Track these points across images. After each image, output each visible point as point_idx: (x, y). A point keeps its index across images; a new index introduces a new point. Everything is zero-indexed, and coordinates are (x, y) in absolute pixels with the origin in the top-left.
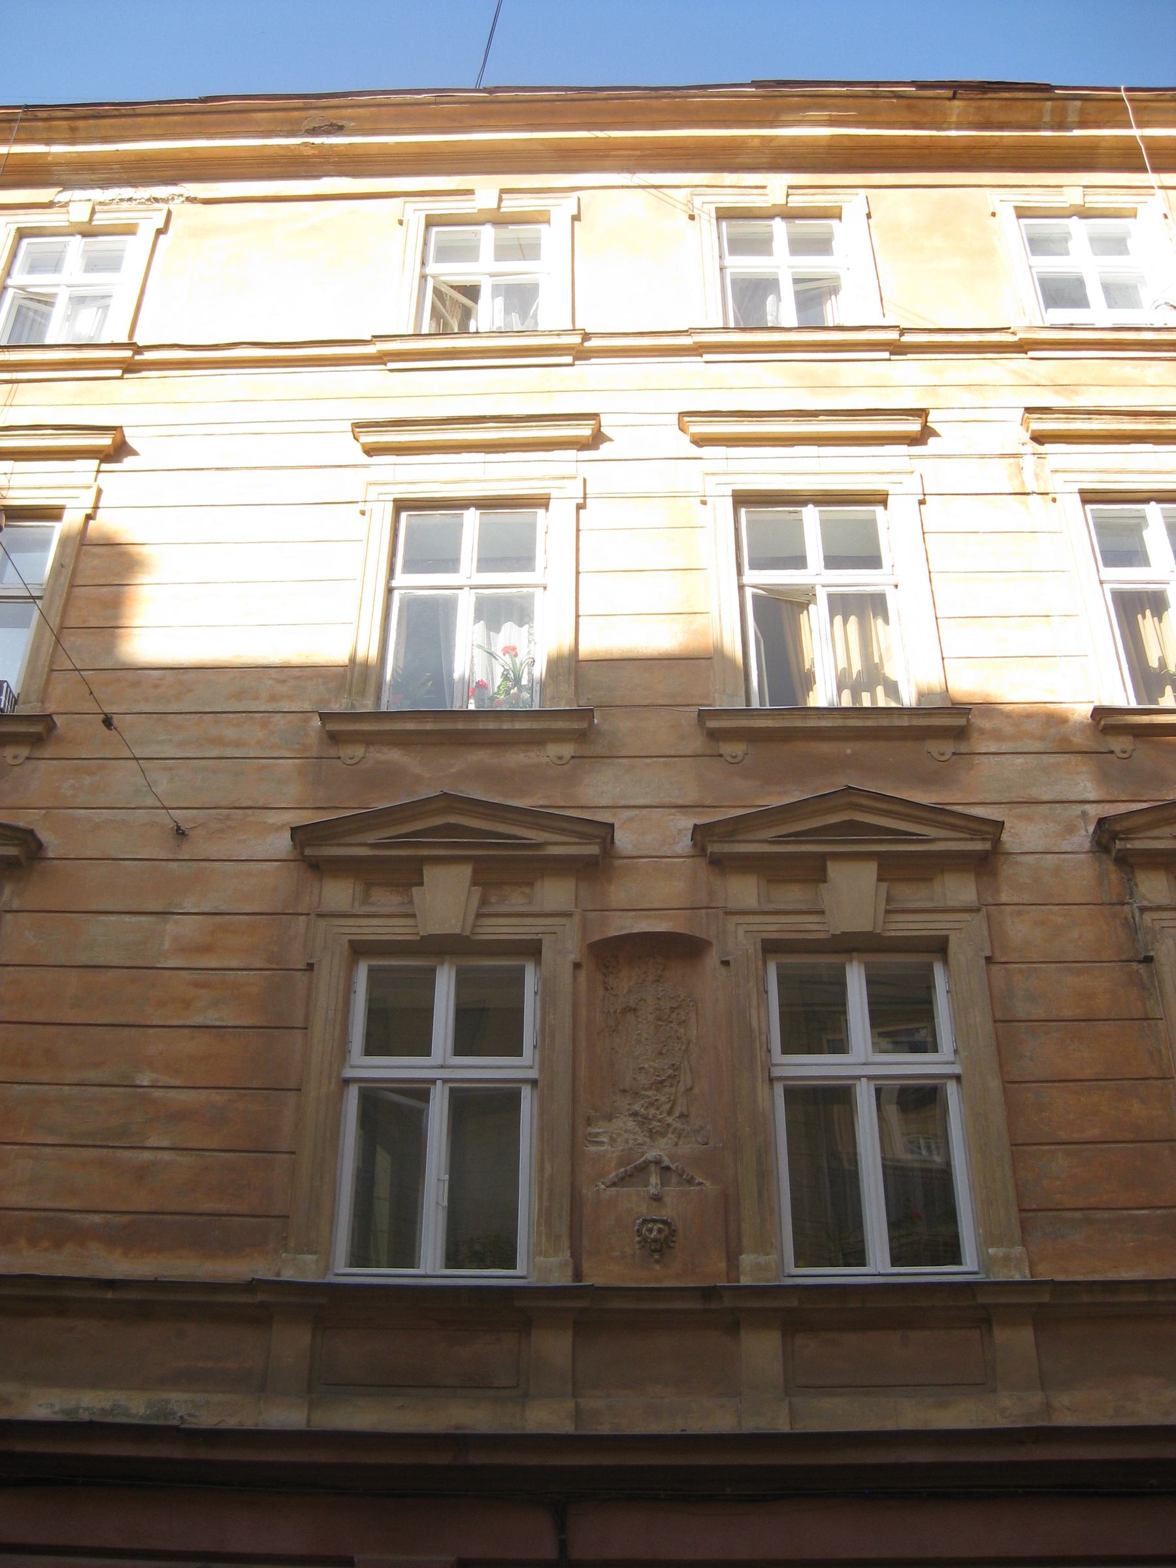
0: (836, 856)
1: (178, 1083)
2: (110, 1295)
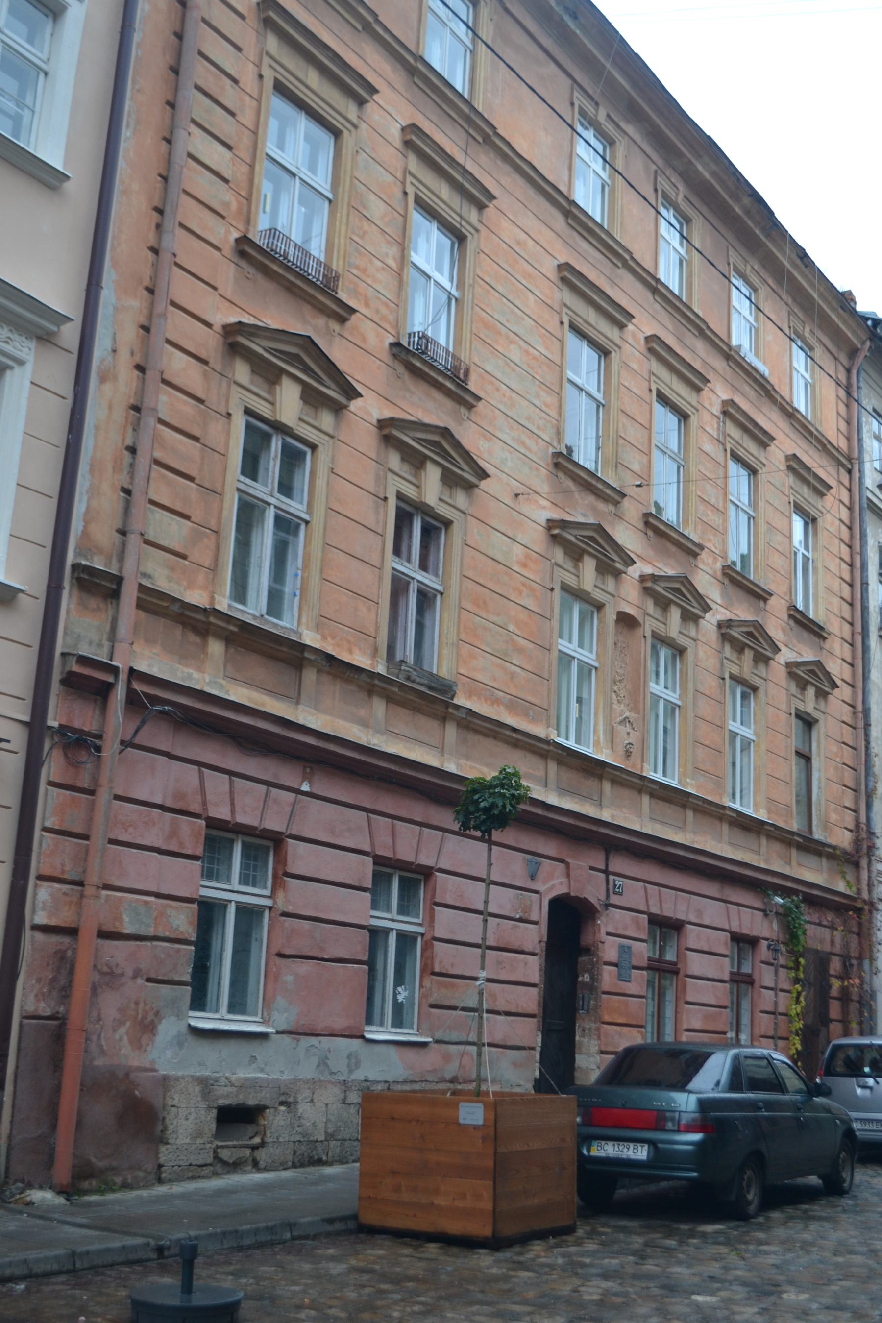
1: (519, 633)
2: (514, 735)
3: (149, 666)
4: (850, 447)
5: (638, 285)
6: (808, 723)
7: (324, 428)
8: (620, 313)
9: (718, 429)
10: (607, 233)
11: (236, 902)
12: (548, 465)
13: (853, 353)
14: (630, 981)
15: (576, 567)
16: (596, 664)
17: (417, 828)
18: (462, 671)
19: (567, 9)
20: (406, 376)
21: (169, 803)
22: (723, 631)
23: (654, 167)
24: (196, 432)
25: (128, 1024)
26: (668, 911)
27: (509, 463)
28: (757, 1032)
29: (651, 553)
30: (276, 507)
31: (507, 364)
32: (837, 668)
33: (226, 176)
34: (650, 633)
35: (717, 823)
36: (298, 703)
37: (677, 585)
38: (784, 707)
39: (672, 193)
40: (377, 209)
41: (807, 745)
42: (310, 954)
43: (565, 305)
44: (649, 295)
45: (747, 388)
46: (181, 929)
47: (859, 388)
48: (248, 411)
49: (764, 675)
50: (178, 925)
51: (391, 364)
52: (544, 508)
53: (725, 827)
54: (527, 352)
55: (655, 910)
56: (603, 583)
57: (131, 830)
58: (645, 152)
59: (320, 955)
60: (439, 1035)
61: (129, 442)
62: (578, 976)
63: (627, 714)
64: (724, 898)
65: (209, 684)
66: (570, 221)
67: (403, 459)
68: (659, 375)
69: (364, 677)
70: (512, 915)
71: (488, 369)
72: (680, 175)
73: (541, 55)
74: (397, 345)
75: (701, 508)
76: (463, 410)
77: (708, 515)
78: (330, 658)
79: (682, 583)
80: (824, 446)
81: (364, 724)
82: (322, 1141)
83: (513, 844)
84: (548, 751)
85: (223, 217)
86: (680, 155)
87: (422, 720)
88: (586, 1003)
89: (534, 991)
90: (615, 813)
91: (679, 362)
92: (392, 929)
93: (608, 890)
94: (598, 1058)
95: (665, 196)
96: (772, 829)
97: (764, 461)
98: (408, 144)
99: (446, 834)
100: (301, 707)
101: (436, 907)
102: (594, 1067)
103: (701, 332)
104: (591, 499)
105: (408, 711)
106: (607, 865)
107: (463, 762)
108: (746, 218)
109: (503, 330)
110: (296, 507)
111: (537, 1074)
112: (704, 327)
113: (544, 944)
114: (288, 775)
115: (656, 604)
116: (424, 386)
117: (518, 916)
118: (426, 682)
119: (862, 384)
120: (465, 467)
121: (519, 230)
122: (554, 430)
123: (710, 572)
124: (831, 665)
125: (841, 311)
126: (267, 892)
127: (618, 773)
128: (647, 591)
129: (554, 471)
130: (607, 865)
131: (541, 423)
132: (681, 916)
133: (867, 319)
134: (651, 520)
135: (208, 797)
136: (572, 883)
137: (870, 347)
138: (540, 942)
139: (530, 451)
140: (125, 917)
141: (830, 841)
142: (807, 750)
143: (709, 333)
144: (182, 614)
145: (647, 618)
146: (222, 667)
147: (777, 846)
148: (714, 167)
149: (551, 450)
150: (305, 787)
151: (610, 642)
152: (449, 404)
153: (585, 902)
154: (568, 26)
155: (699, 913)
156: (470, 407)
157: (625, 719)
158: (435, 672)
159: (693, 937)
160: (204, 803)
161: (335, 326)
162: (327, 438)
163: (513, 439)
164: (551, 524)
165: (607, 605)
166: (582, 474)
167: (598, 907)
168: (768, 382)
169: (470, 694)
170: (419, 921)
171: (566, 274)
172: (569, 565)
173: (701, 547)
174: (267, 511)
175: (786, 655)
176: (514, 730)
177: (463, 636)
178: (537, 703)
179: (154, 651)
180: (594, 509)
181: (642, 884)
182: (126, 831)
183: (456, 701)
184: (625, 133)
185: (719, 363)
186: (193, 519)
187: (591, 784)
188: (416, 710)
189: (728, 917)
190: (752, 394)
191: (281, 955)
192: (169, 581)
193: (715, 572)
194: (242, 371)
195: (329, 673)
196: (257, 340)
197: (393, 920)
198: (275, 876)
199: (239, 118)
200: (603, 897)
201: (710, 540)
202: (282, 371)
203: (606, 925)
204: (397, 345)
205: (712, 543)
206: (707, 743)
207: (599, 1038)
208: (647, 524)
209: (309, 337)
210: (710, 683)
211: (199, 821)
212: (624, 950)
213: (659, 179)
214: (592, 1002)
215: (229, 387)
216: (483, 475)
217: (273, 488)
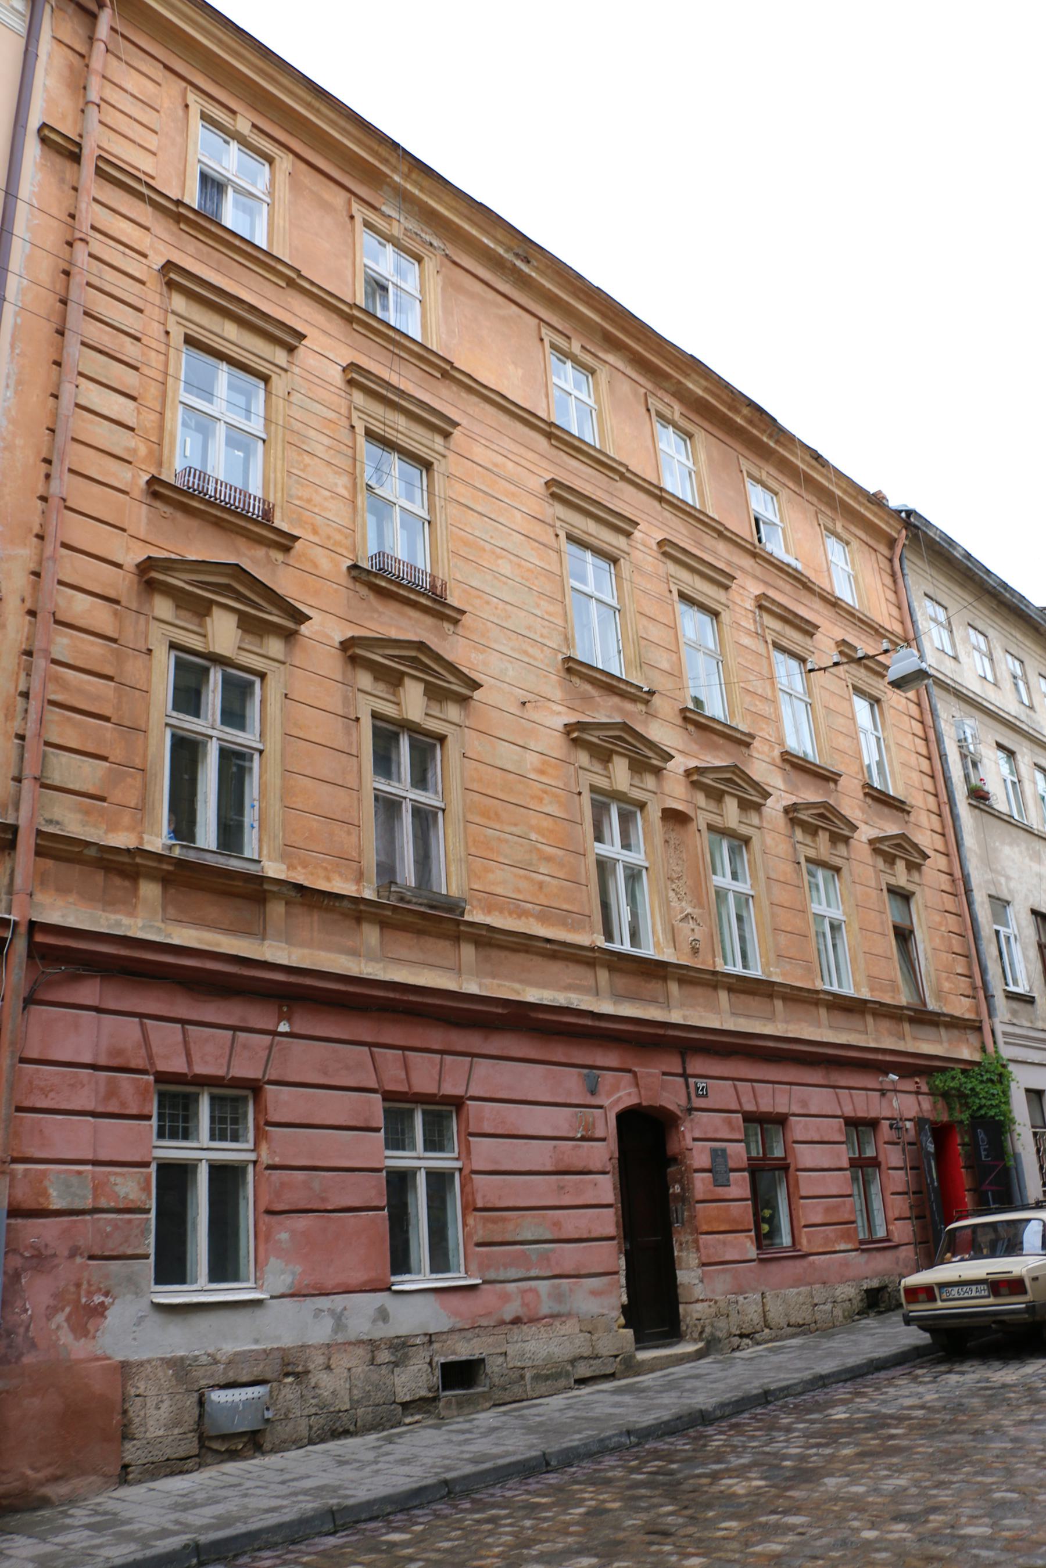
1: (544, 841)
2: (548, 946)
3: (63, 916)
4: (905, 630)
5: (643, 497)
6: (903, 896)
7: (271, 654)
8: (623, 522)
9: (755, 621)
10: (600, 451)
11: (207, 1160)
12: (558, 671)
13: (891, 543)
15: (606, 768)
16: (646, 864)
17: (437, 1057)
18: (475, 887)
19: (517, 255)
20: (372, 597)
21: (103, 1061)
22: (791, 816)
23: (643, 391)
24: (108, 671)
25: (68, 1310)
26: (766, 1106)
27: (511, 673)
28: (890, 1215)
29: (694, 747)
30: (219, 739)
31: (497, 578)
32: (925, 840)
33: (130, 424)
34: (705, 826)
35: (813, 1009)
36: (263, 939)
37: (728, 775)
38: (873, 884)
39: (667, 412)
40: (319, 443)
41: (908, 918)
42: (309, 1207)
43: (558, 518)
44: (656, 504)
45: (781, 583)
46: (131, 1197)
47: (903, 575)
48: (173, 646)
49: (845, 854)
50: (127, 1194)
51: (351, 586)
52: (559, 713)
53: (823, 1012)
54: (519, 565)
55: (749, 1107)
56: (642, 782)
57: (52, 1095)
58: (630, 377)
59: (322, 1207)
60: (492, 1275)
61: (22, 687)
62: (668, 1189)
63: (689, 910)
64: (832, 1084)
65: (143, 928)
66: (553, 442)
67: (376, 679)
68: (678, 576)
69: (346, 903)
70: (571, 1135)
71: (473, 584)
72: (674, 395)
73: (500, 299)
74: (355, 567)
75: (748, 699)
76: (446, 625)
77: (756, 705)
78: (299, 888)
79: (734, 773)
80: (876, 631)
81: (354, 953)
82: (346, 1411)
83: (563, 1060)
84: (595, 958)
85: (130, 463)
86: (667, 377)
87: (430, 942)
88: (680, 1216)
89: (612, 1210)
90: (687, 1013)
91: (698, 563)
92: (420, 1168)
93: (689, 1094)
94: (700, 1271)
95: (659, 415)
96: (877, 1006)
97: (812, 649)
98: (351, 382)
99: (475, 1059)
100: (267, 943)
101: (471, 1139)
102: (697, 1281)
103: (720, 534)
104: (616, 700)
105: (410, 935)
106: (684, 1068)
107: (487, 981)
108: (750, 428)
109: (488, 546)
110: (246, 738)
111: (624, 1299)
112: (722, 529)
113: (615, 1162)
114: (258, 1016)
115: (708, 796)
116: (396, 606)
117: (579, 1135)
118: (425, 901)
119: (906, 571)
120: (452, 679)
121: (495, 454)
122: (562, 637)
123: (768, 760)
124: (920, 837)
125: (869, 505)
126: (250, 1145)
127: (684, 972)
128: (695, 784)
129: (567, 677)
130: (684, 1068)
131: (545, 631)
132: (782, 1109)
133: (901, 511)
134: (689, 714)
135: (155, 1050)
136: (643, 1092)
137: (907, 536)
138: (610, 1159)
139: (535, 659)
140: (51, 1191)
141: (945, 1010)
142: (908, 923)
143: (729, 534)
144: (102, 859)
145: (699, 811)
146: (160, 910)
147: (885, 1024)
148: (704, 383)
149: (560, 657)
150: (284, 1027)
151: (658, 839)
152: (429, 621)
153: (662, 1109)
154: (521, 270)
155: (804, 1103)
156: (456, 622)
157: (686, 916)
158: (444, 892)
159: (799, 1128)
160: (150, 1057)
161: (278, 556)
162: (276, 664)
163: (512, 649)
164: (569, 728)
165: (649, 803)
166: (598, 676)
167: (679, 1113)
168: (802, 574)
169: (489, 910)
170: (456, 1155)
171: (554, 489)
172: (597, 767)
173: (752, 736)
174: (209, 745)
175: (865, 833)
176: (548, 941)
177: (473, 851)
178: (575, 910)
179: (71, 900)
180: (620, 710)
181: (731, 1082)
182: (47, 1096)
183: (467, 918)
184: (606, 362)
185: (747, 562)
186: (111, 759)
187: (654, 987)
188: (420, 932)
189: (839, 1103)
190: (788, 588)
191: (269, 1212)
192: (84, 826)
193: (773, 759)
194: (163, 607)
195: (302, 904)
196: (177, 574)
197: (419, 1158)
198: (257, 1128)
199: (145, 370)
200: (683, 1102)
201: (762, 729)
202: (212, 602)
203: (692, 1131)
204: (355, 567)
205: (764, 731)
206: (789, 929)
207: (698, 1250)
208: (685, 719)
209: (237, 565)
210: (783, 869)
211: (146, 1077)
212: (717, 1155)
213: (650, 400)
214: (686, 1214)
215: (147, 623)
216: (476, 685)
217: (214, 720)
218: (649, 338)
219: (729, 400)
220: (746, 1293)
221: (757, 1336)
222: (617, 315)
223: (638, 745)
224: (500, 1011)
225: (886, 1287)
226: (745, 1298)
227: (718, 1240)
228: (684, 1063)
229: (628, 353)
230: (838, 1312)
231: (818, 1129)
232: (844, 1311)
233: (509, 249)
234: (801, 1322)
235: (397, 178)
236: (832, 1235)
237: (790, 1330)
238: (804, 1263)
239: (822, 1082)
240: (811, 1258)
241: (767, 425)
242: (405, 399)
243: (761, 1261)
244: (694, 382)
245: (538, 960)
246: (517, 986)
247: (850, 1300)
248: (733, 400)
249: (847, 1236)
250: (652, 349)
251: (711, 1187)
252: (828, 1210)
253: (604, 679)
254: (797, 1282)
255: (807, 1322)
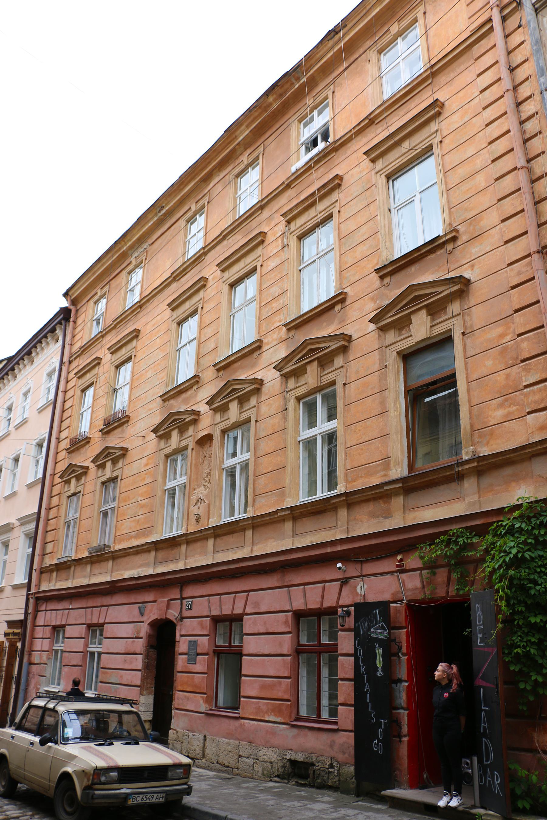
0: (230, 401)
2: (131, 550)
14: (195, 664)
19: (160, 211)
26: (227, 610)
64: (285, 584)
86: (233, 151)
89: (140, 673)
91: (238, 253)
93: (181, 608)
106: (181, 595)
123: (275, 343)
139: (152, 409)
148: (243, 127)
150: (70, 607)
159: (249, 624)
166: (172, 393)
167: (175, 621)
176: (131, 548)
212: (193, 644)
218: (209, 156)
219: (259, 111)
220: (195, 732)
221: (196, 761)
222: (194, 172)
223: (181, 417)
224: (108, 586)
225: (313, 764)
226: (194, 735)
227: (185, 696)
228: (181, 591)
229: (215, 171)
230: (259, 768)
231: (265, 623)
232: (263, 770)
233: (156, 214)
234: (226, 764)
235: (124, 248)
236: (264, 708)
237: (218, 766)
238: (237, 723)
239: (277, 584)
240: (243, 721)
241: (287, 82)
242: (122, 341)
243: (207, 714)
244: (241, 133)
245: (132, 557)
246: (122, 572)
247: (271, 763)
248: (260, 108)
249: (278, 711)
250: (216, 156)
251: (186, 664)
252: (263, 687)
253: (174, 392)
254: (229, 735)
255: (230, 765)
